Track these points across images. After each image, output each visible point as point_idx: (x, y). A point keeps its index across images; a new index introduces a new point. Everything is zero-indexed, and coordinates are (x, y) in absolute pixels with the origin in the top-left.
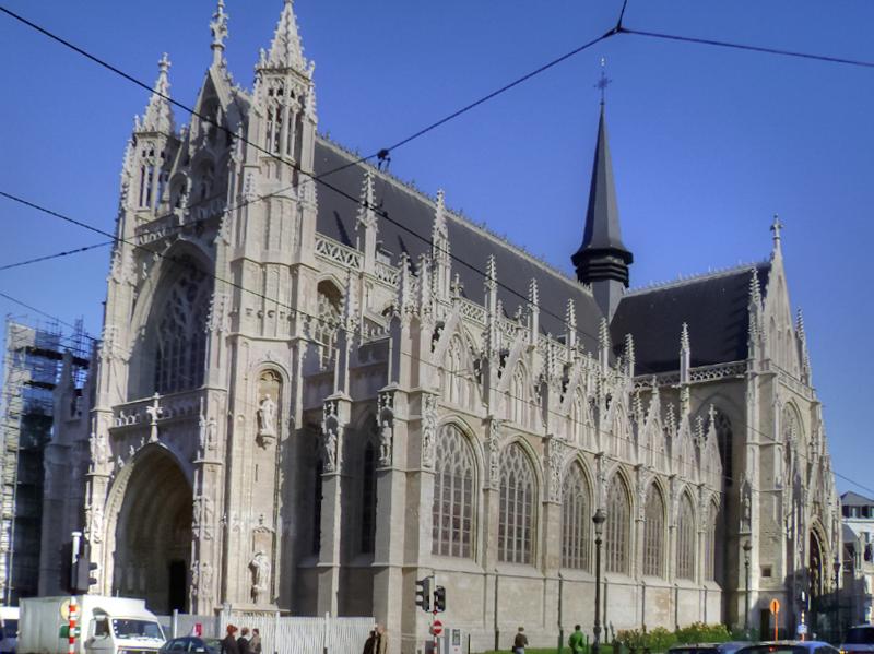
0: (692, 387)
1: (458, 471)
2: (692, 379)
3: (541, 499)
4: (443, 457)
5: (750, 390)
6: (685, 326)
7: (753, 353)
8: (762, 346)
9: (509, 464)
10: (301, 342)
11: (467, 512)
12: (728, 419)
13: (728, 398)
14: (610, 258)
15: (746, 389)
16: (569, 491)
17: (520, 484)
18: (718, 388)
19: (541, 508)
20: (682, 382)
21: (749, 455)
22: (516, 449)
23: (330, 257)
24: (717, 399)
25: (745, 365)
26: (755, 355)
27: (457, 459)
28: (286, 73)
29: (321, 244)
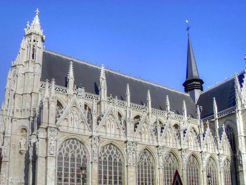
0: (219, 119)
1: (79, 156)
2: (219, 116)
3: (126, 164)
4: (70, 152)
5: (237, 116)
6: (214, 98)
7: (237, 103)
8: (241, 100)
9: (108, 152)
10: (31, 117)
11: (120, 173)
12: (232, 129)
13: (231, 121)
14: (194, 82)
15: (236, 116)
16: (144, 160)
17: (115, 160)
18: (228, 118)
19: (126, 168)
20: (215, 118)
21: (240, 140)
22: (112, 147)
23: (61, 92)
24: (228, 122)
25: (235, 108)
26: (239, 103)
27: (78, 151)
28: (32, 35)
29: (57, 88)
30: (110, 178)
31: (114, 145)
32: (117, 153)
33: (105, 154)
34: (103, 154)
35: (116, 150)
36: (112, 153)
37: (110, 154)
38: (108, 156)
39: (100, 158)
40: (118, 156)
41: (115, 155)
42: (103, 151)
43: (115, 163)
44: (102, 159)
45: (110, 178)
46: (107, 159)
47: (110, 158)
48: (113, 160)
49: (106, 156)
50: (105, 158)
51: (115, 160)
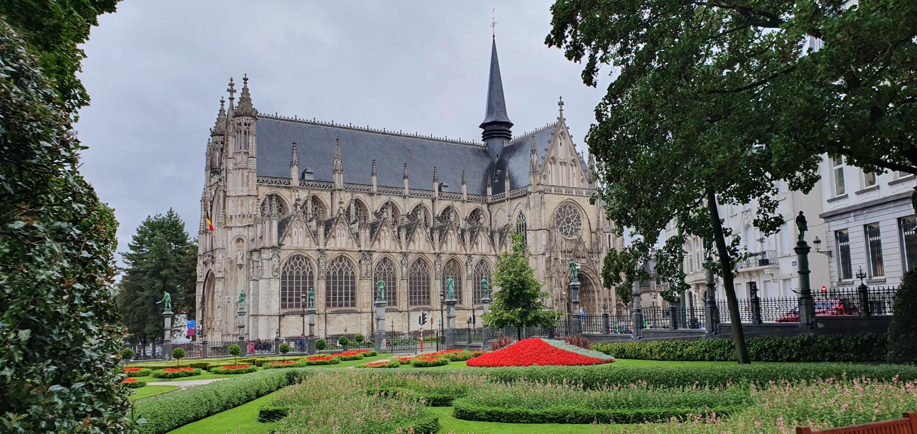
9: (338, 266)
17: (347, 273)
18: (520, 200)
30: (341, 294)
31: (345, 257)
32: (349, 265)
33: (335, 267)
34: (332, 268)
35: (348, 262)
36: (343, 265)
37: (341, 267)
38: (338, 270)
39: (329, 272)
40: (350, 268)
41: (347, 267)
42: (332, 264)
43: (347, 277)
44: (332, 273)
45: (341, 294)
46: (337, 273)
47: (341, 272)
48: (344, 273)
49: (336, 270)
50: (335, 273)
51: (347, 273)
